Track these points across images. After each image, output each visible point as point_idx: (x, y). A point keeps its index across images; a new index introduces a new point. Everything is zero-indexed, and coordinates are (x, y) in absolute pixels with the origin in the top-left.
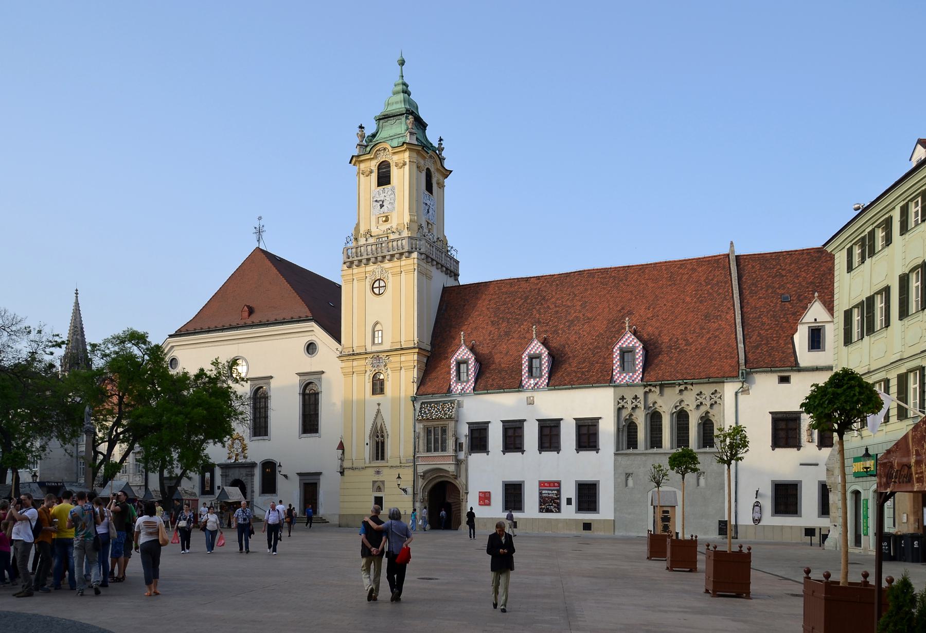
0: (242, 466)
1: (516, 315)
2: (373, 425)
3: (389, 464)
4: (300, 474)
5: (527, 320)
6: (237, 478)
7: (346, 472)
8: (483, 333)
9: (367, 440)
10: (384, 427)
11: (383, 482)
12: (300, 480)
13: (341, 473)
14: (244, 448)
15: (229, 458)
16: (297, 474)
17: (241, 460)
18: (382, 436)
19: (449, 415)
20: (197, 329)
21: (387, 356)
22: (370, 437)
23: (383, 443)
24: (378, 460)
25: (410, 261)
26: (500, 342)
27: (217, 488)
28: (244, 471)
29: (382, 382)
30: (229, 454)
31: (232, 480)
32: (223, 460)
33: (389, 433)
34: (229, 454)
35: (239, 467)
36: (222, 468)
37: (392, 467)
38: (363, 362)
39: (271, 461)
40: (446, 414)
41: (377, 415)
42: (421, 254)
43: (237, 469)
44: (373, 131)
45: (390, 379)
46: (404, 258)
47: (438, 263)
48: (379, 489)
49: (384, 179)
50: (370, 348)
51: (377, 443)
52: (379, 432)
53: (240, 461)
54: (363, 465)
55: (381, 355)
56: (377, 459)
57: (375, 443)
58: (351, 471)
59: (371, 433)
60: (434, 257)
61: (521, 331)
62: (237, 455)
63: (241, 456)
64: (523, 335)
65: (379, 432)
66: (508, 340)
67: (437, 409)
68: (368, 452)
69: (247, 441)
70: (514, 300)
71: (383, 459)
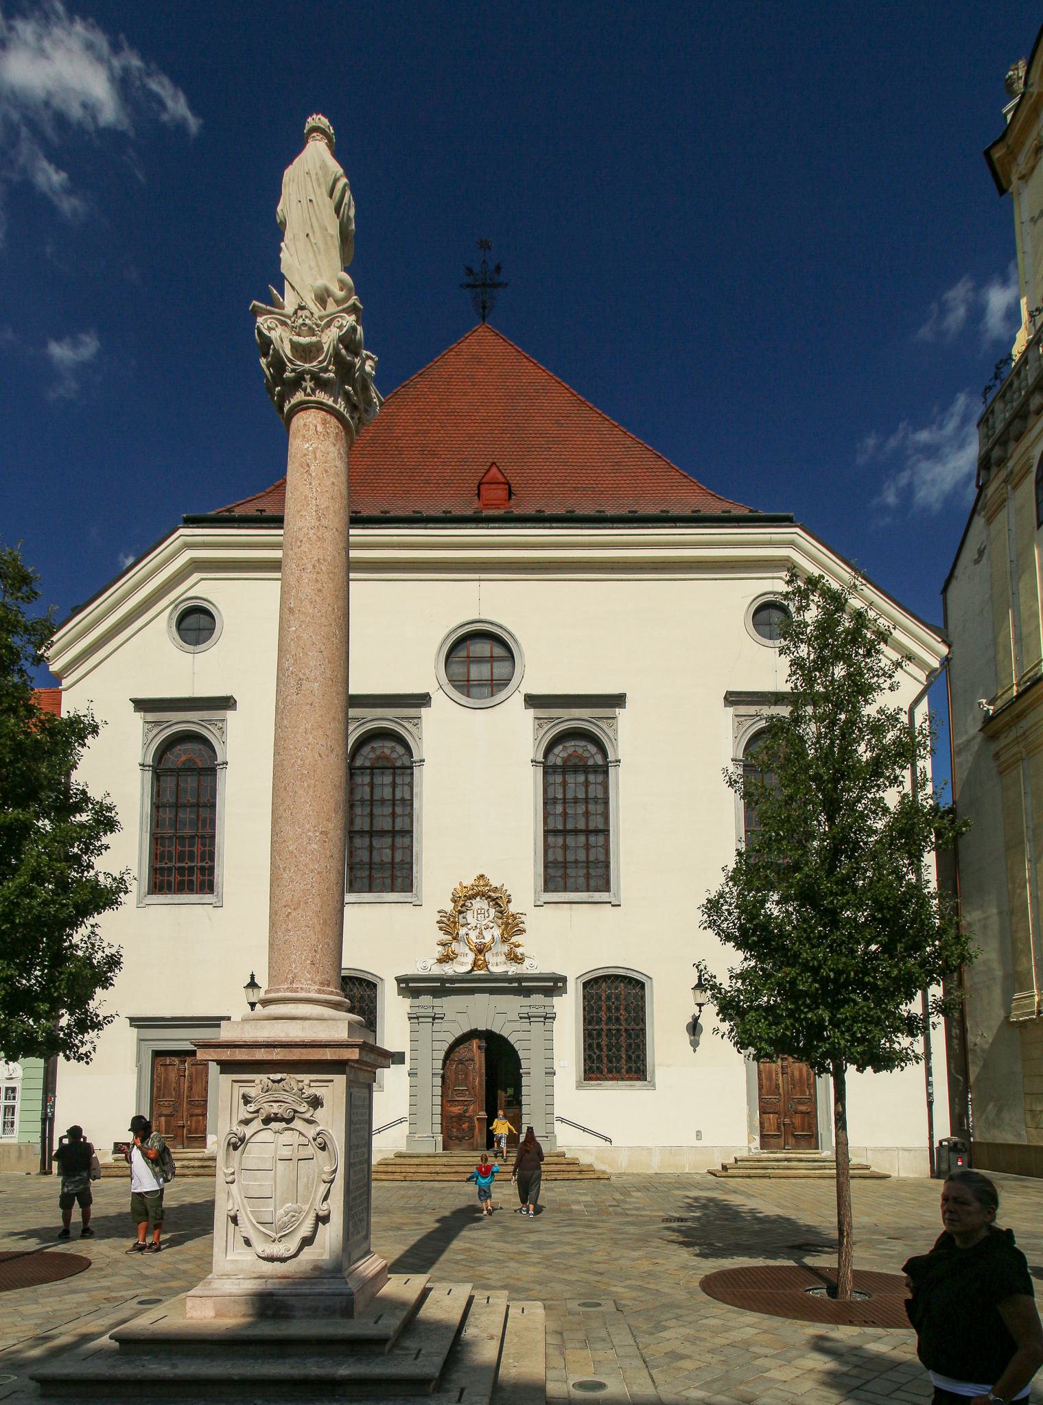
0: (521, 986)
14: (511, 926)
15: (445, 959)
17: (498, 965)
28: (513, 1004)
39: (622, 972)
53: (494, 969)
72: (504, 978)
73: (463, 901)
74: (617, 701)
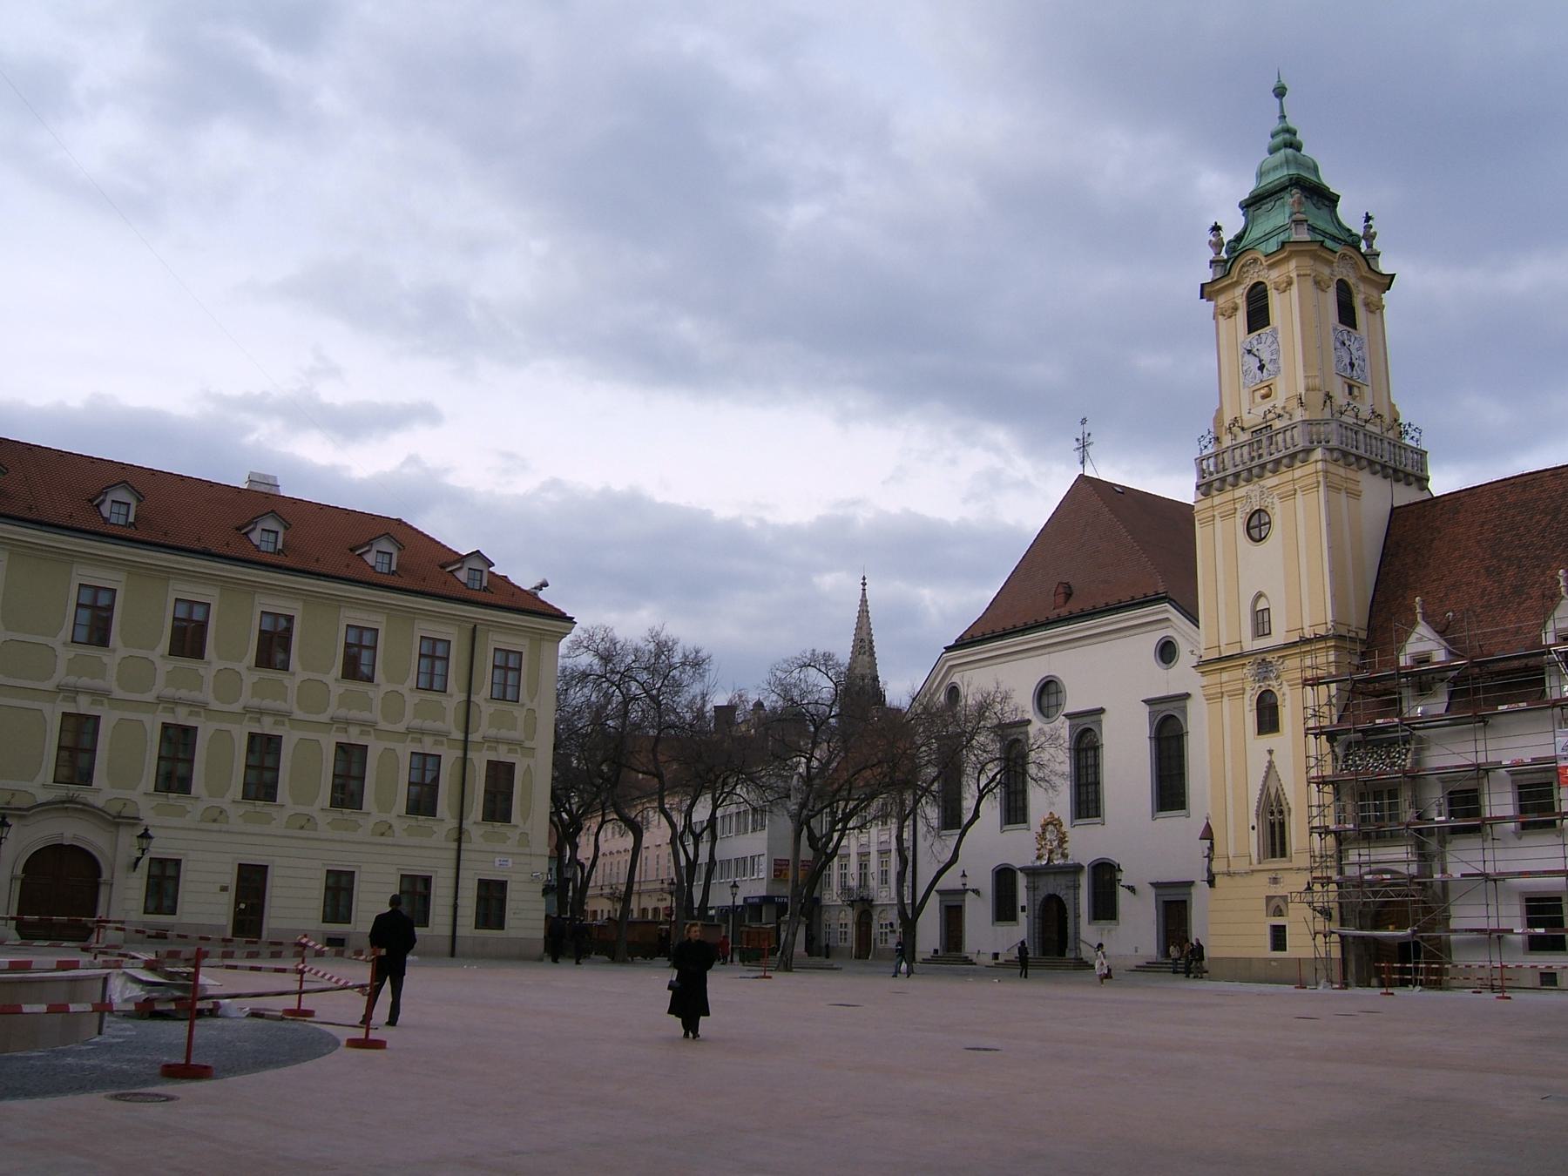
1: (1536, 550)
2: (1262, 790)
3: (1295, 864)
4: (1156, 885)
5: (1558, 556)
6: (1052, 893)
7: (1218, 879)
8: (1468, 593)
9: (1253, 821)
10: (1281, 795)
11: (1284, 898)
12: (1156, 895)
13: (1208, 882)
14: (1062, 841)
15: (1039, 857)
16: (1151, 884)
18: (1281, 812)
19: (1400, 765)
20: (996, 631)
21: (1279, 657)
22: (1258, 815)
23: (1282, 825)
24: (1275, 857)
25: (1310, 469)
26: (1503, 609)
27: (1020, 909)
28: (1063, 881)
29: (1274, 709)
30: (1038, 850)
31: (1043, 896)
32: (1030, 861)
33: (1292, 805)
34: (1038, 850)
35: (1055, 873)
36: (1027, 875)
37: (1299, 869)
38: (1238, 673)
40: (1394, 764)
41: (1267, 773)
42: (1331, 450)
43: (1052, 877)
44: (1238, 229)
45: (1287, 703)
46: (1298, 464)
47: (1371, 463)
48: (1279, 912)
49: (1258, 316)
50: (1250, 644)
51: (1272, 825)
52: (1274, 804)
53: (1056, 862)
54: (1247, 868)
55: (1269, 658)
56: (1274, 856)
57: (1268, 823)
58: (1227, 878)
59: (1258, 807)
60: (1361, 452)
61: (1545, 581)
62: (1051, 852)
63: (1057, 854)
64: (1550, 589)
65: (1274, 804)
66: (1519, 604)
67: (1378, 755)
68: (1253, 842)
69: (1066, 827)
70: (1531, 519)
71: (1283, 855)
72: (1059, 867)
73: (1044, 827)
74: (1102, 711)
